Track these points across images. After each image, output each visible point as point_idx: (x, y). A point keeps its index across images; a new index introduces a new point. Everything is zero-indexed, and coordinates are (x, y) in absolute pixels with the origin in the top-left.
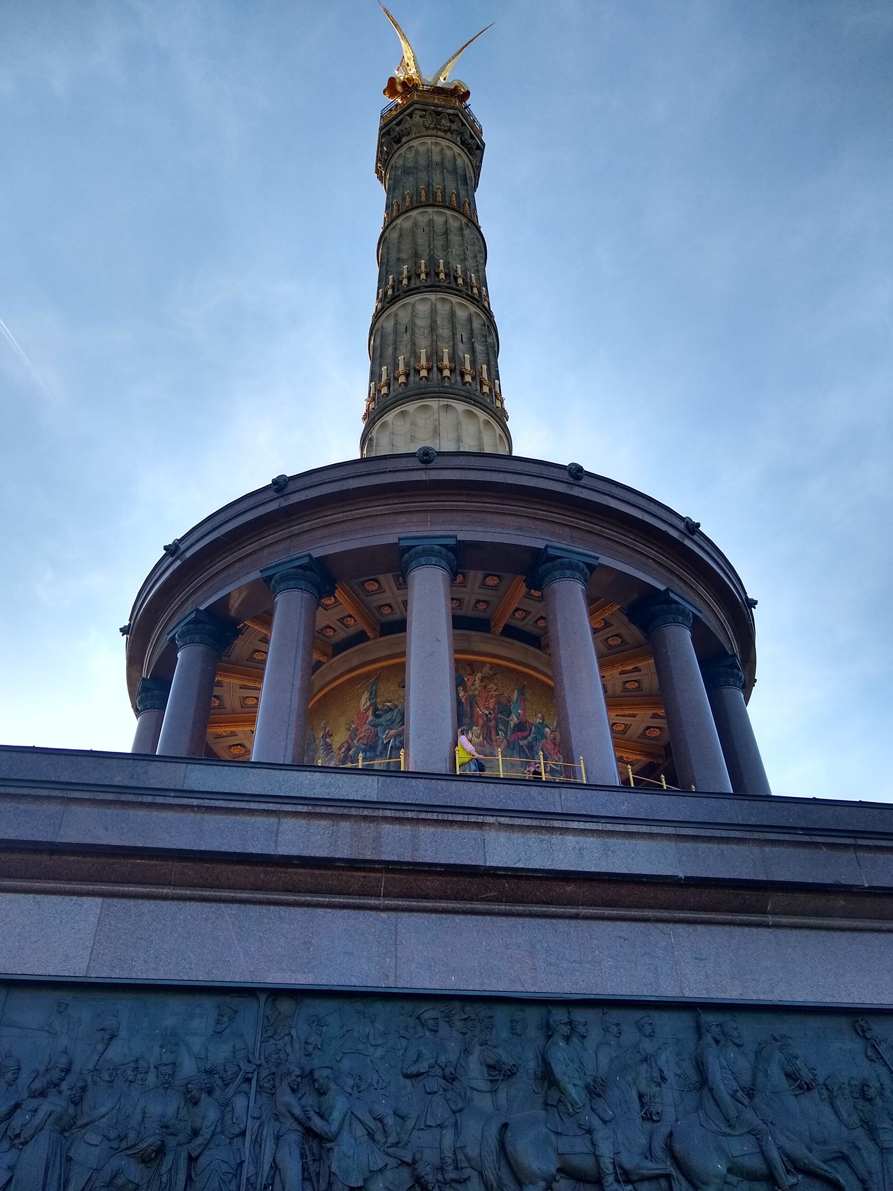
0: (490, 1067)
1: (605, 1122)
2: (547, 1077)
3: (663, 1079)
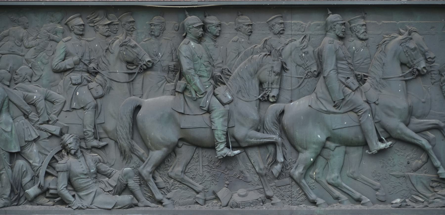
0: (128, 63)
1: (223, 104)
2: (177, 71)
3: (284, 68)
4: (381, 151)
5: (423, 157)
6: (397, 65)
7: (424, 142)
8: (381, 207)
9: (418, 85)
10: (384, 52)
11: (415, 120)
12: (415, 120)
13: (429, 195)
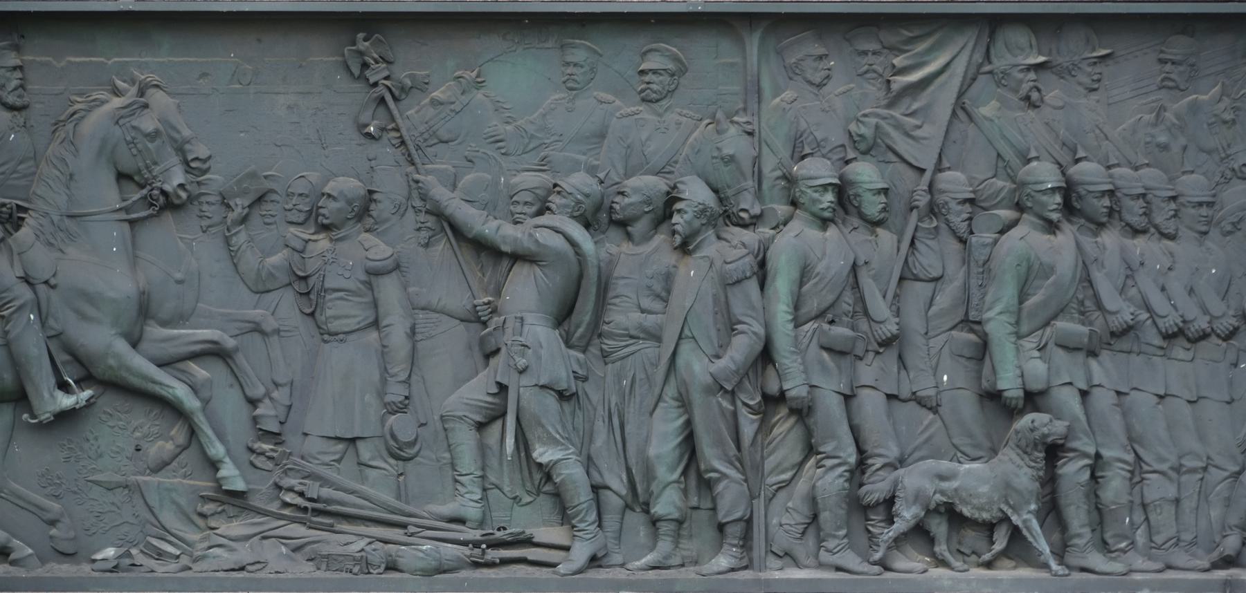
4: (65, 417)
5: (178, 433)
6: (108, 178)
7: (180, 391)
8: (64, 569)
9: (165, 234)
10: (72, 143)
11: (155, 331)
12: (155, 331)
13: (193, 536)
